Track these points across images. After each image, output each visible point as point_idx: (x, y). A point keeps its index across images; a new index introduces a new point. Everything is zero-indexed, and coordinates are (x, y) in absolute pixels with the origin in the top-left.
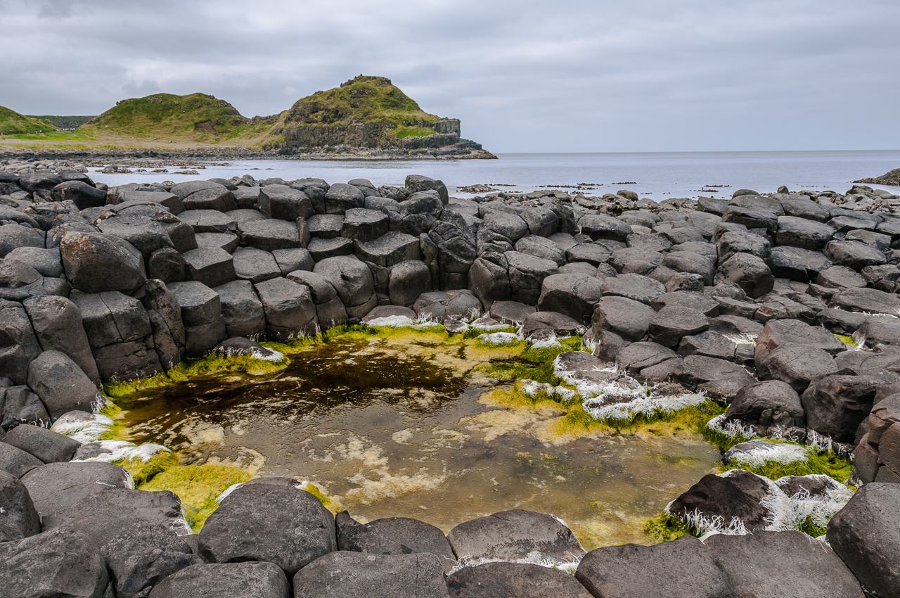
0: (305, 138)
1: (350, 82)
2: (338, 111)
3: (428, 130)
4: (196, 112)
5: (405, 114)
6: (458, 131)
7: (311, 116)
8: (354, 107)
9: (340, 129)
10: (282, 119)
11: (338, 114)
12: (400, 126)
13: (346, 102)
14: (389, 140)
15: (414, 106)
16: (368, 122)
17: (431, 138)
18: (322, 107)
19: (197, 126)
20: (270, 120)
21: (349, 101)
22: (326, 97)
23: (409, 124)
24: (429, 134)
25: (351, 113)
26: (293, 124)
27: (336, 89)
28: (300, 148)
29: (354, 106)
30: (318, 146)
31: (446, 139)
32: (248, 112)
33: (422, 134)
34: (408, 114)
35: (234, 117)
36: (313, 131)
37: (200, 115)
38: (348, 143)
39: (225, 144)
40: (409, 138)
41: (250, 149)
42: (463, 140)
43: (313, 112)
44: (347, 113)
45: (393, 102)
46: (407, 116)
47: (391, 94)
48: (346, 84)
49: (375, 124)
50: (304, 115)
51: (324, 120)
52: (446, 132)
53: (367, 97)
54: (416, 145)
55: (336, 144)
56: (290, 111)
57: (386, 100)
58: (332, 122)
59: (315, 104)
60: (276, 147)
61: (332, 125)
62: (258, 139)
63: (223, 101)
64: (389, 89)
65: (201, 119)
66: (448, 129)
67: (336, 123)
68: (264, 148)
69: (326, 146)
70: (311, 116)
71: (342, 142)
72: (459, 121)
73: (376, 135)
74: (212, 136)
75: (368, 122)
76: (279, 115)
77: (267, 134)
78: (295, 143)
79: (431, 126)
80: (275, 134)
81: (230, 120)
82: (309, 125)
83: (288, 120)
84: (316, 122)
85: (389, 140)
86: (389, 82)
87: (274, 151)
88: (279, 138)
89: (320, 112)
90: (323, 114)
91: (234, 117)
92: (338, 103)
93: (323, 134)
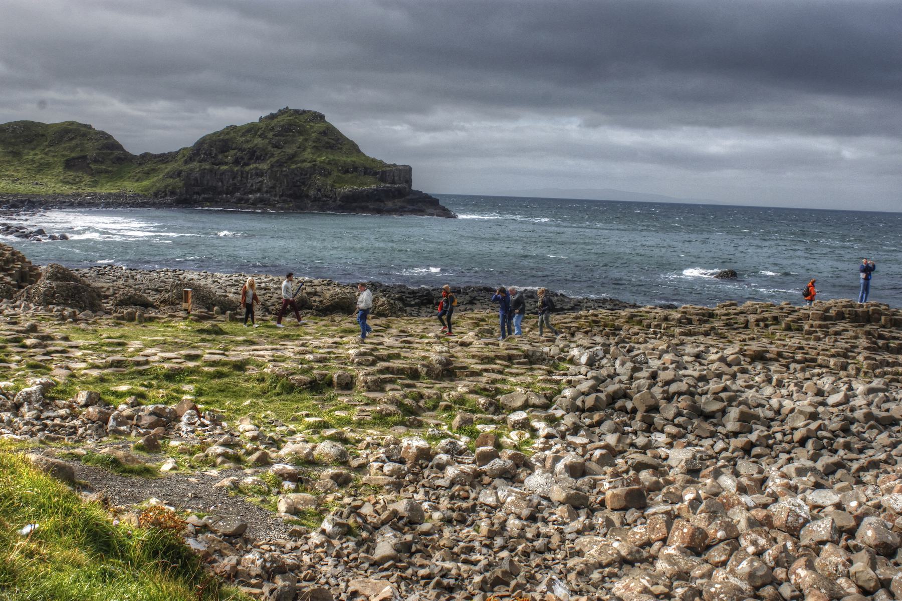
0: (210, 184)
1: (272, 117)
2: (255, 152)
3: (370, 179)
4: (67, 145)
5: (344, 159)
6: (409, 181)
7: (220, 157)
8: (277, 147)
9: (257, 175)
11: (255, 155)
12: (335, 174)
13: (267, 141)
14: (319, 190)
15: (353, 148)
16: (294, 166)
17: (375, 190)
18: (234, 146)
19: (69, 165)
20: (164, 158)
21: (271, 140)
22: (240, 134)
23: (346, 172)
24: (372, 185)
25: (272, 155)
26: (195, 165)
27: (252, 124)
28: (203, 196)
29: (276, 146)
30: (227, 194)
31: (391, 192)
33: (362, 184)
34: (345, 159)
35: (116, 153)
36: (222, 174)
37: (72, 149)
38: (267, 192)
39: (106, 189)
40: (346, 189)
41: (138, 195)
43: (222, 152)
44: (266, 154)
45: (328, 143)
46: (345, 162)
47: (324, 133)
48: (266, 118)
49: (303, 170)
50: (210, 154)
51: (236, 162)
52: (393, 182)
53: (294, 136)
55: (250, 193)
56: (191, 149)
57: (318, 140)
58: (248, 165)
59: (225, 142)
60: (173, 193)
61: (247, 168)
62: (145, 183)
63: (103, 133)
64: (318, 126)
65: (73, 155)
66: (396, 178)
67: (251, 166)
68: (156, 195)
69: (238, 194)
70: (220, 157)
71: (259, 190)
73: (303, 183)
74: (87, 179)
75: (294, 166)
76: (177, 153)
77: (161, 177)
78: (197, 189)
79: (375, 173)
80: (171, 177)
81: (112, 157)
82: (216, 167)
83: (190, 160)
84: (226, 164)
85: (319, 190)
86: (322, 117)
87: (169, 199)
88: (178, 182)
89: (232, 152)
90: (235, 155)
91: (116, 153)
92: (256, 142)
93: (233, 179)
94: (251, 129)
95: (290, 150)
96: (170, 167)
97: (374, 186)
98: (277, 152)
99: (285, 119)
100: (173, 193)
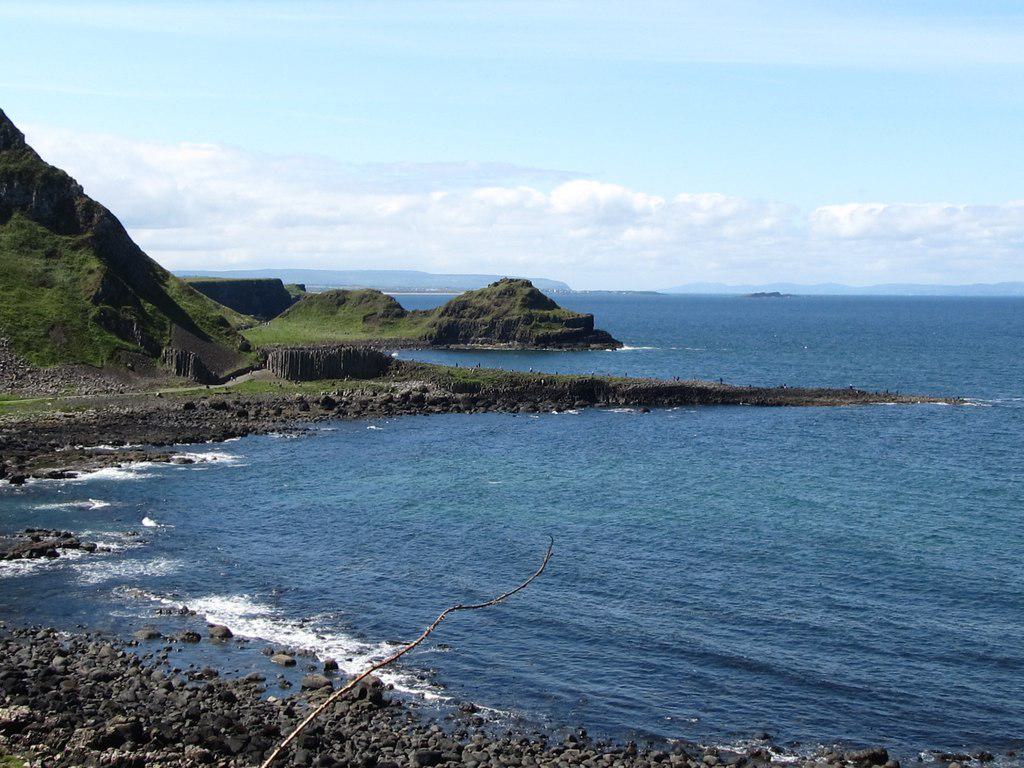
1: (496, 284)
10: (436, 315)
11: (483, 311)
15: (552, 305)
16: (506, 319)
20: (426, 313)
26: (445, 318)
32: (408, 308)
40: (541, 332)
42: (597, 331)
54: (545, 341)
61: (478, 320)
69: (472, 338)
72: (592, 316)
74: (377, 329)
83: (442, 315)
86: (528, 284)
94: (482, 294)
95: (505, 307)
96: (429, 320)
97: (560, 330)
98: (497, 308)
99: (502, 287)
100: (430, 338)
